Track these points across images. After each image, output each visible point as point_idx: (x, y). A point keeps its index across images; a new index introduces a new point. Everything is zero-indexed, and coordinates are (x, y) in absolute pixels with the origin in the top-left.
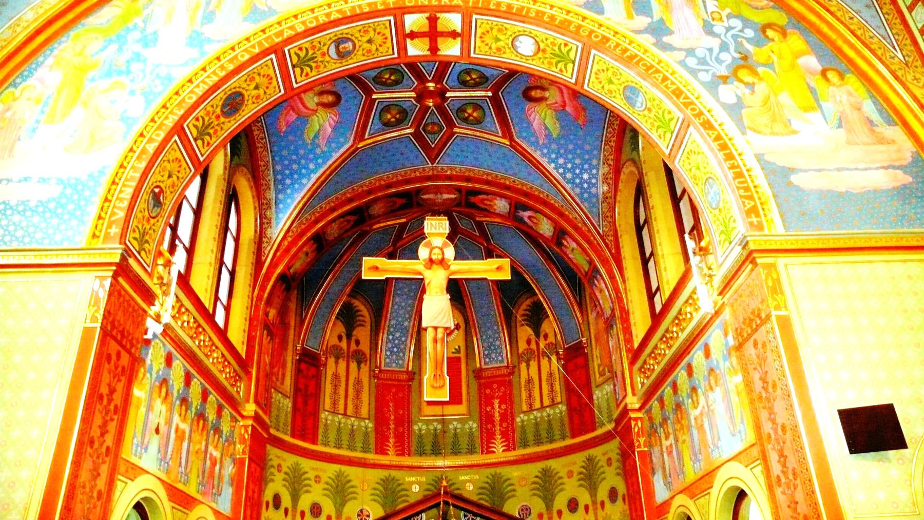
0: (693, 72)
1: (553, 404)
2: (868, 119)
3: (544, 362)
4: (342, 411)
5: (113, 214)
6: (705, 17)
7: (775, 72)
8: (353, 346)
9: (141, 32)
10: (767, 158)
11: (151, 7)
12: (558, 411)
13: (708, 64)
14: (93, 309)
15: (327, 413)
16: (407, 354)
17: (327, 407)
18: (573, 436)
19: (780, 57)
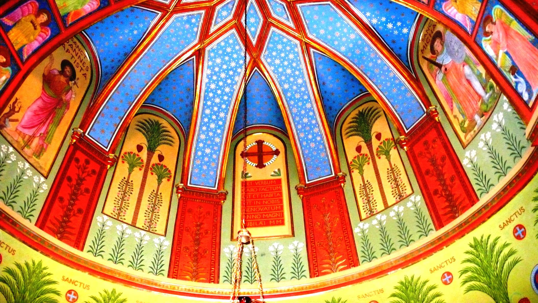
1: (401, 198)
4: (129, 220)
8: (155, 160)
15: (106, 217)
17: (110, 208)
18: (439, 225)
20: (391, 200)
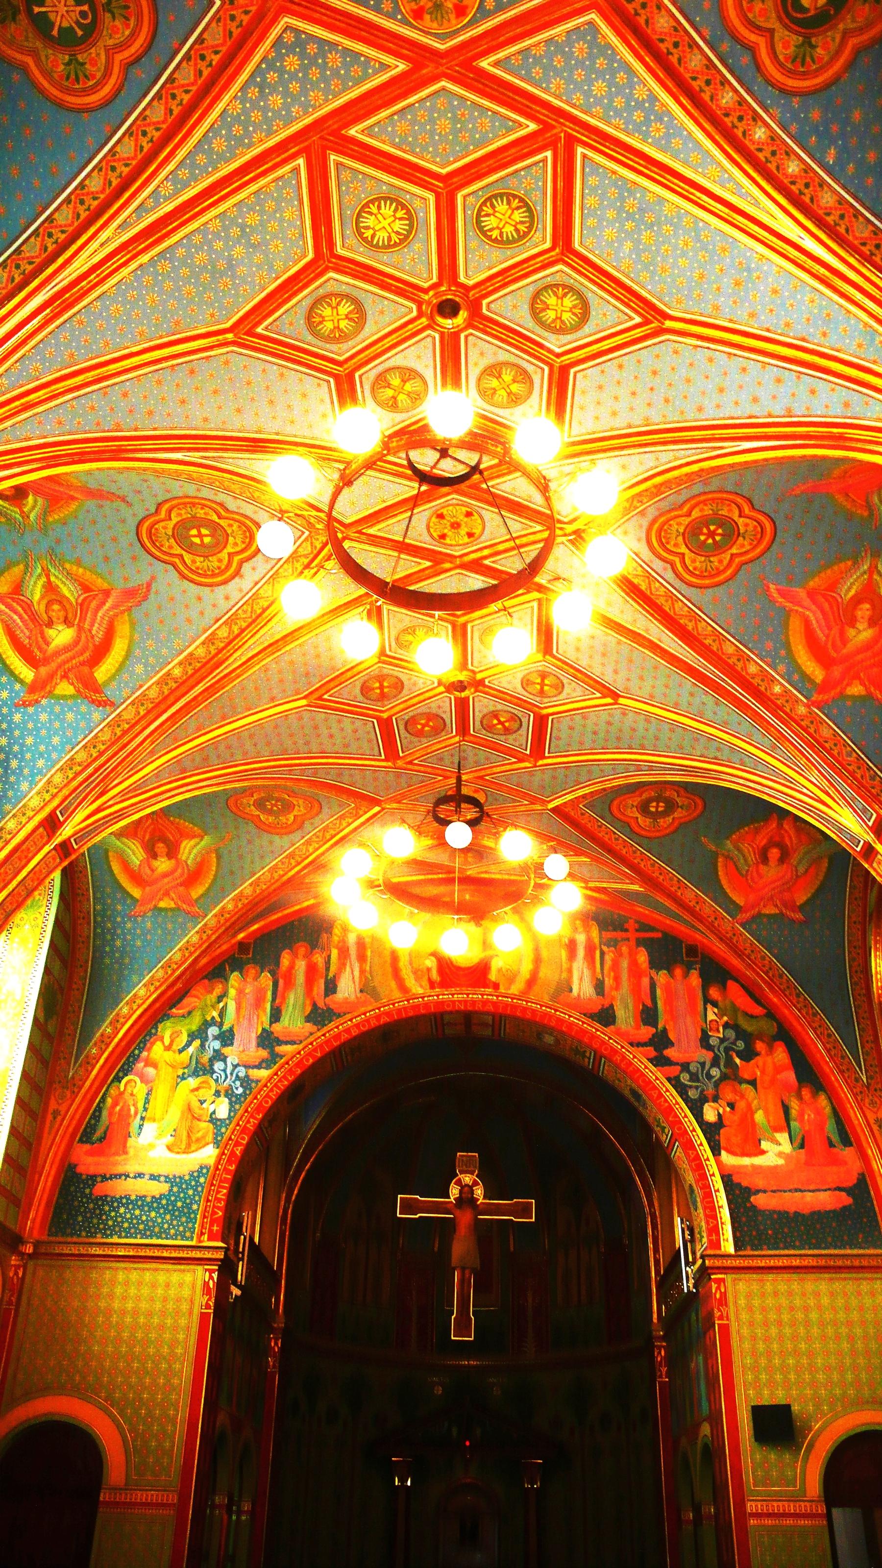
0: (682, 1090)
2: (828, 1138)
5: (214, 1213)
10: (736, 1179)
11: (225, 999)
14: (206, 1298)
19: (763, 1072)
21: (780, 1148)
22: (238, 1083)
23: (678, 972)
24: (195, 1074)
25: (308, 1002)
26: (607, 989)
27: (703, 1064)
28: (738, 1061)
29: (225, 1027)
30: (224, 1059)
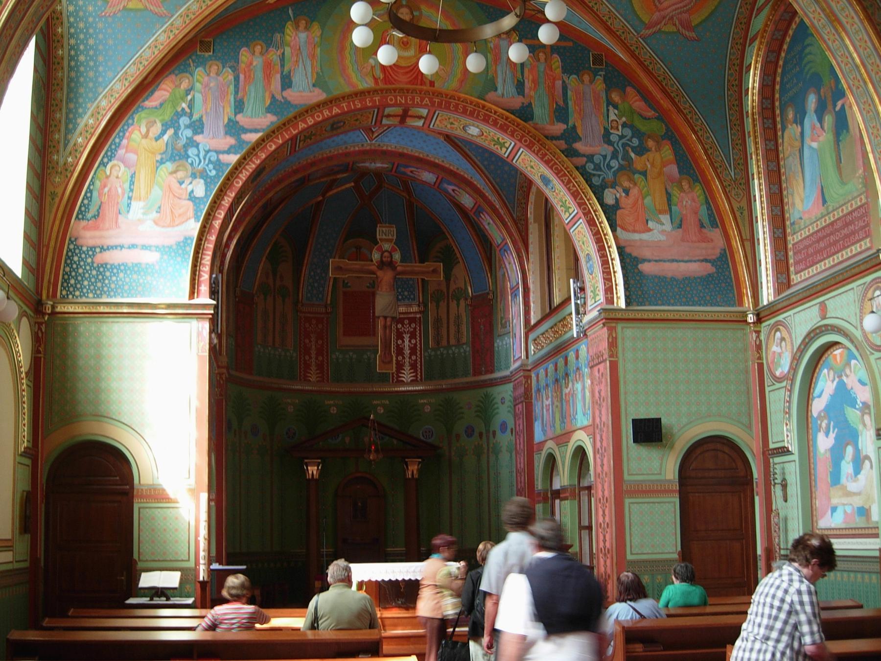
3: (453, 305)
6: (606, 126)
7: (646, 179)
9: (189, 117)
10: (628, 250)
12: (462, 350)
13: (601, 170)
16: (326, 289)
19: (653, 165)
20: (453, 341)
21: (664, 227)
22: (211, 166)
23: (586, 78)
24: (172, 159)
25: (267, 95)
26: (526, 91)
27: (605, 157)
28: (633, 155)
29: (196, 117)
30: (197, 146)
